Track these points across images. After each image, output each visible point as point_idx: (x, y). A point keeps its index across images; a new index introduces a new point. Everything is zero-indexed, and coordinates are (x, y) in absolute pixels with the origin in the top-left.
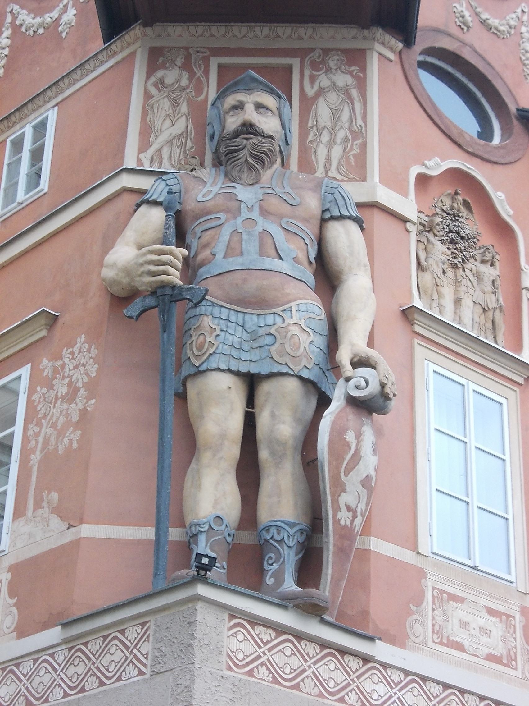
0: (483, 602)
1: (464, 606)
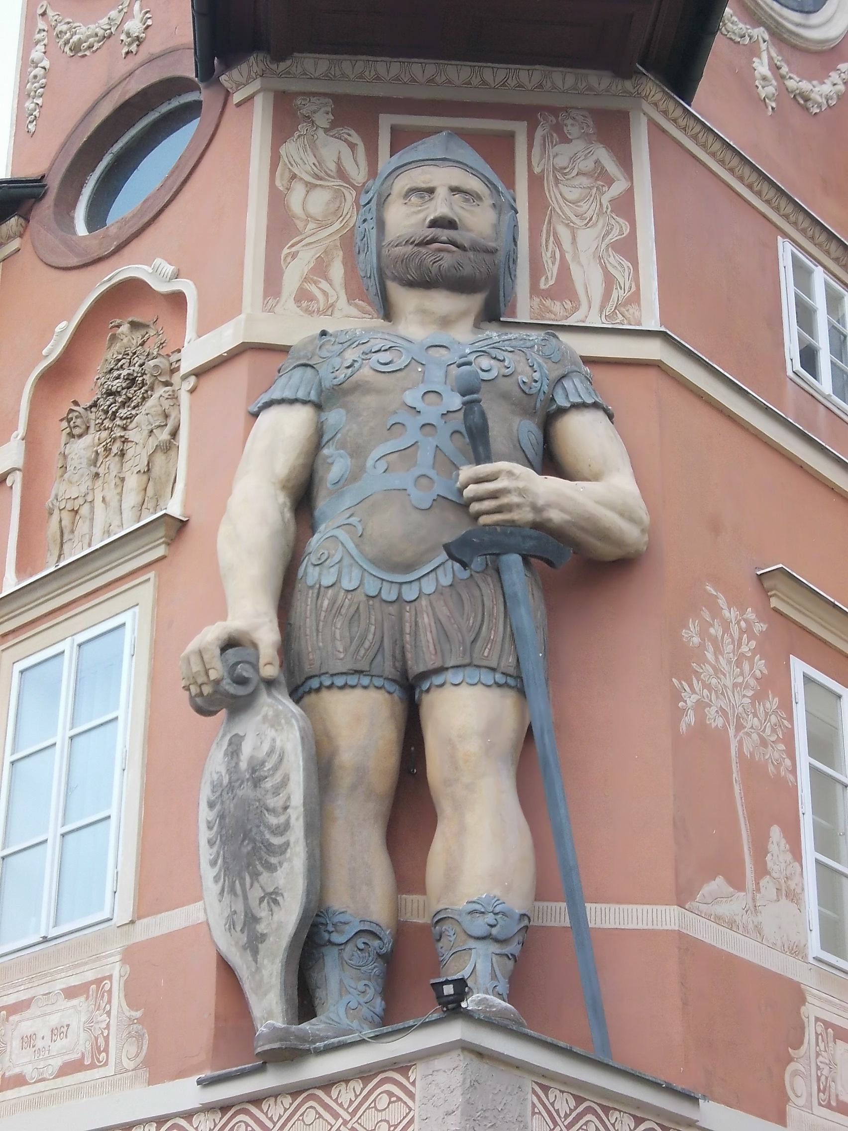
0: (60, 985)
1: (33, 1010)
